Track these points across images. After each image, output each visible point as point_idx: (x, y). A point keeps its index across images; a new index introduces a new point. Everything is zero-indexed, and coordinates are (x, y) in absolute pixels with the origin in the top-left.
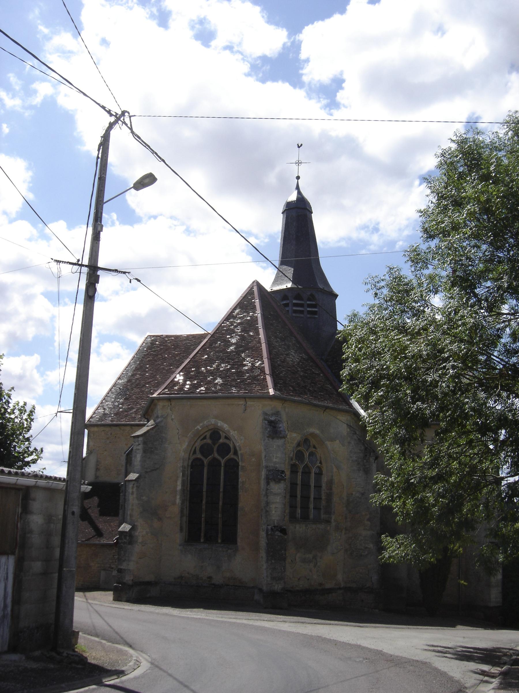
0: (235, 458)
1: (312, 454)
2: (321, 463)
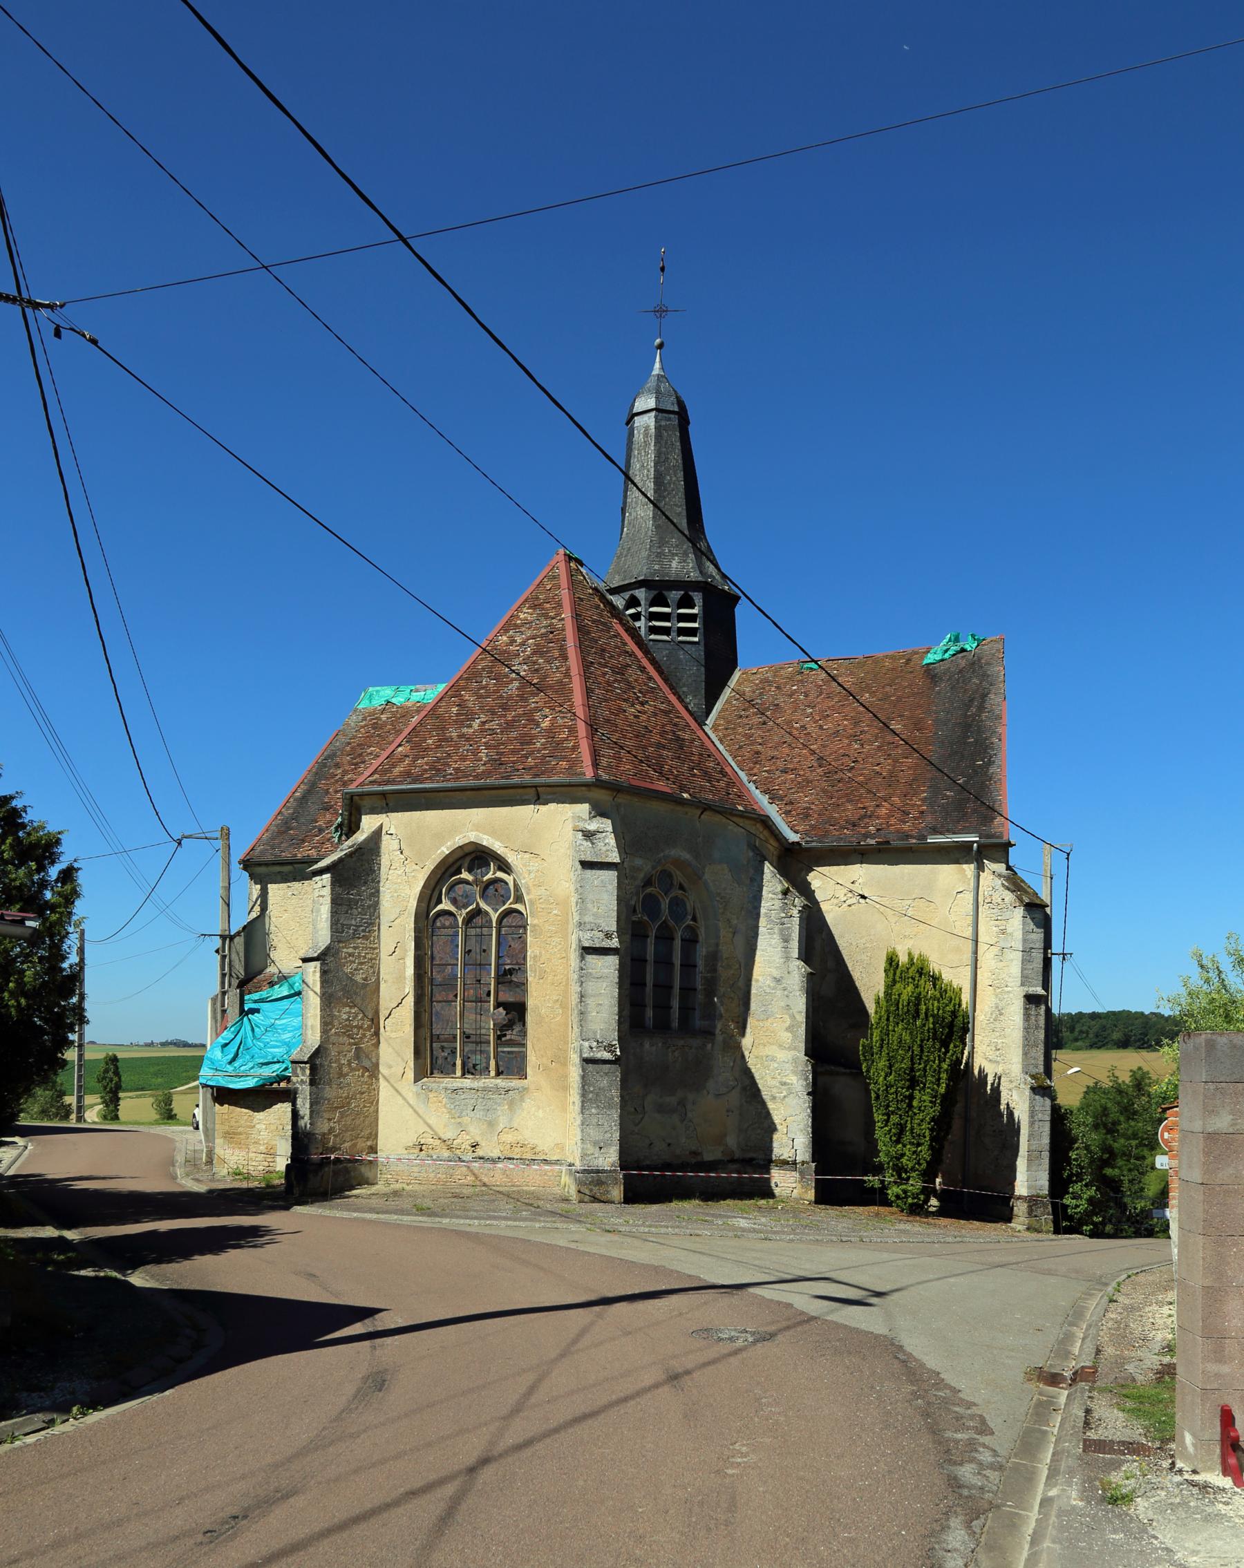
0: (518, 906)
1: (677, 904)
2: (694, 919)
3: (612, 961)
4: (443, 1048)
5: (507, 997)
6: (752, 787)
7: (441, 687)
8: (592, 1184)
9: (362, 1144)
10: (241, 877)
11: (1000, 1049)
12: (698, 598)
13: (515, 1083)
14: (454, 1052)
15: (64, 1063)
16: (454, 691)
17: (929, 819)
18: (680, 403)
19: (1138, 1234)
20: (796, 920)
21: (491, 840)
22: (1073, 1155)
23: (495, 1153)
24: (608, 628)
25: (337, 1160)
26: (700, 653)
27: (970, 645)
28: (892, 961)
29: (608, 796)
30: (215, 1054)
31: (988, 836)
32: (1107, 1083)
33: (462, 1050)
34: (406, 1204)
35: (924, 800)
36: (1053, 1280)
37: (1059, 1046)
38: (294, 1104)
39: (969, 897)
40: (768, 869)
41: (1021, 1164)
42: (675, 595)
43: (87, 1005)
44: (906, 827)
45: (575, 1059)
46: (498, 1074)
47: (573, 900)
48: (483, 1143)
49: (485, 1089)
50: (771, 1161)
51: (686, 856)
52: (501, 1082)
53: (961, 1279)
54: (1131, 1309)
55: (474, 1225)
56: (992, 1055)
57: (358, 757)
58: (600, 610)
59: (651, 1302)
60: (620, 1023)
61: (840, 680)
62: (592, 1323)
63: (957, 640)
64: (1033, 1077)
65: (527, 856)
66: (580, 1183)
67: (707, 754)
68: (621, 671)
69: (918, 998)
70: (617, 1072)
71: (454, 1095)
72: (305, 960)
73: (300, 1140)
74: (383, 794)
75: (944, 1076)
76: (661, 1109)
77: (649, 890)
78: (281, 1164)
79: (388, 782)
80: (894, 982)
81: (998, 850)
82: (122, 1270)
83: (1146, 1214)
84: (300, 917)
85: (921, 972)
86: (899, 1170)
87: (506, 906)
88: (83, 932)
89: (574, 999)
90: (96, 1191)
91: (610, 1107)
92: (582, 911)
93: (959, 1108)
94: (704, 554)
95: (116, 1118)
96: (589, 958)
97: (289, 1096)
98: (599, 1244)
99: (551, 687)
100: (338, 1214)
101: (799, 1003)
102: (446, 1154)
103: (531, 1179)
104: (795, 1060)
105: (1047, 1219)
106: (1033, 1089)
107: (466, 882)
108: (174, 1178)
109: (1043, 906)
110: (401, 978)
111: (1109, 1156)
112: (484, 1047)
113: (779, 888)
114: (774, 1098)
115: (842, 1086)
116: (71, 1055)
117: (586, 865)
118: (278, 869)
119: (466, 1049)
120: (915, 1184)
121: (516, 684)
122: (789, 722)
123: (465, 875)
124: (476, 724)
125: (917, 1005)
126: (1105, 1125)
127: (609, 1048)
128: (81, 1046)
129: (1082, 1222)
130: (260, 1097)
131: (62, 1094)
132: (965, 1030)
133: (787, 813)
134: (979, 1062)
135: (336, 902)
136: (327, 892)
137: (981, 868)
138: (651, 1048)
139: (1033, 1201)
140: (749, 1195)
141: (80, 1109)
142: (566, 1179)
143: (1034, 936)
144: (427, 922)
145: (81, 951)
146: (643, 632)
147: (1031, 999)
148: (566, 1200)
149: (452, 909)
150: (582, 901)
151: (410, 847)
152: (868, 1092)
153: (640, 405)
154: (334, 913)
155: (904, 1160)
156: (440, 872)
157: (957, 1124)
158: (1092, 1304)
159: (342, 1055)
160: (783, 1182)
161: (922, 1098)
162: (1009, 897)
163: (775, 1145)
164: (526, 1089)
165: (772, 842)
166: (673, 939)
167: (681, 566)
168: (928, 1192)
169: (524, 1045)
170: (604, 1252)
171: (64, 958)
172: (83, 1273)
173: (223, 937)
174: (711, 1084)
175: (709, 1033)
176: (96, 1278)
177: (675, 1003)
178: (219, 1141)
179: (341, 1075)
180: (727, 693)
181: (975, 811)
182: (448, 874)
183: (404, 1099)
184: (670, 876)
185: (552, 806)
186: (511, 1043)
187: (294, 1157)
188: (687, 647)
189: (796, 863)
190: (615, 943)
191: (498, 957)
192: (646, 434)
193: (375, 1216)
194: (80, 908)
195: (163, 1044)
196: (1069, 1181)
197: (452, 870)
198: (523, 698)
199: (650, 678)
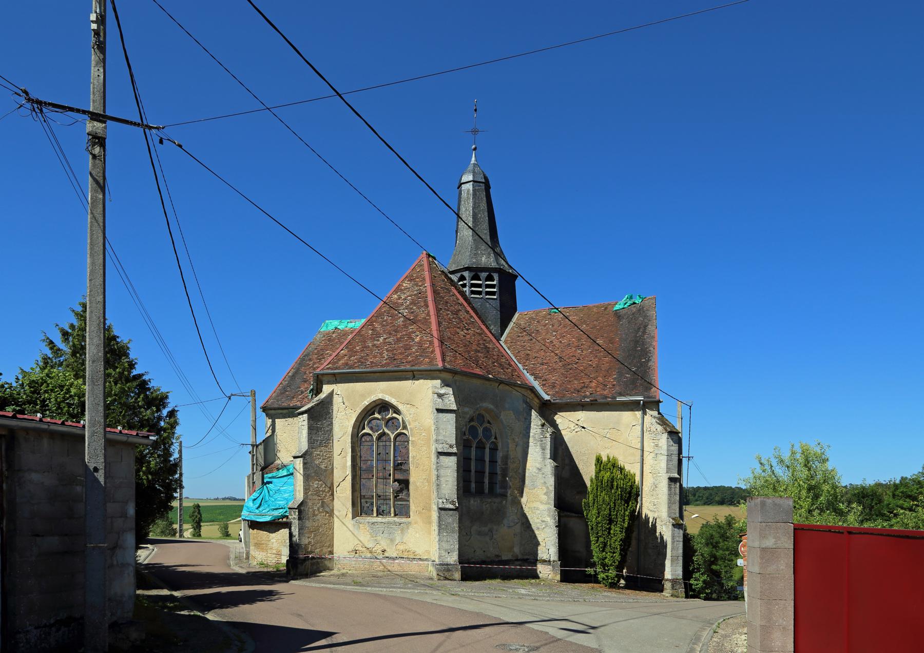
0: (404, 431)
1: (486, 430)
2: (496, 438)
3: (454, 459)
5: (399, 476)
6: (525, 372)
7: (363, 321)
8: (444, 571)
9: (325, 550)
10: (261, 415)
11: (656, 505)
12: (496, 276)
13: (404, 520)
14: (372, 504)
15: (172, 508)
16: (370, 322)
17: (617, 388)
18: (486, 178)
19: (729, 599)
20: (549, 439)
22: (695, 559)
23: (394, 555)
24: (449, 291)
25: (313, 558)
26: (497, 304)
27: (638, 301)
28: (599, 460)
29: (449, 376)
30: (249, 504)
31: (649, 397)
32: (713, 523)
34: (349, 580)
35: (615, 379)
36: (684, 621)
37: (687, 503)
38: (290, 530)
39: (639, 428)
40: (534, 414)
41: (668, 563)
42: (484, 275)
43: (184, 479)
44: (605, 392)
45: (435, 508)
46: (396, 515)
47: (433, 428)
48: (388, 550)
49: (388, 523)
50: (537, 560)
51: (491, 407)
52: (396, 519)
53: (637, 620)
54: (725, 636)
55: (384, 591)
56: (652, 508)
57: (321, 356)
58: (446, 282)
59: (477, 630)
60: (458, 490)
61: (571, 318)
62: (445, 641)
63: (631, 298)
64: (673, 519)
66: (438, 570)
67: (501, 355)
68: (456, 313)
69: (613, 479)
70: (456, 515)
72: (295, 457)
73: (294, 548)
74: (334, 374)
75: (627, 518)
76: (480, 533)
77: (472, 424)
78: (284, 559)
79: (336, 368)
80: (600, 470)
81: (655, 404)
82: (203, 611)
83: (733, 589)
84: (292, 436)
85: (614, 466)
86: (604, 565)
88: (181, 443)
89: (434, 478)
90: (189, 572)
91: (453, 532)
92: (438, 434)
93: (635, 535)
94: (499, 255)
95: (200, 535)
96: (441, 457)
97: (288, 525)
98: (448, 601)
99: (420, 321)
100: (314, 585)
101: (551, 481)
102: (369, 555)
103: (413, 568)
104: (549, 510)
105: (681, 591)
106: (673, 525)
107: (378, 419)
108: (229, 566)
109: (677, 433)
110: (344, 467)
111: (714, 560)
113: (540, 423)
114: (538, 528)
115: (574, 523)
116: (176, 504)
117: (439, 411)
118: (280, 411)
120: (612, 573)
121: (402, 319)
122: (544, 339)
123: (377, 415)
124: (381, 339)
125: (612, 482)
126: (712, 544)
127: (452, 503)
128: (181, 499)
129: (700, 592)
130: (273, 526)
131: (172, 523)
132: (638, 495)
133: (544, 385)
134: (645, 511)
135: (310, 428)
136: (306, 423)
137: (645, 413)
138: (474, 503)
139: (674, 582)
140: (527, 578)
141: (181, 531)
142: (431, 568)
143: (673, 448)
144: (357, 439)
145: (180, 452)
146: (467, 294)
147: (671, 480)
148: (431, 579)
149: (370, 432)
150: (437, 428)
151: (348, 402)
152: (587, 526)
153: (464, 179)
154: (309, 434)
155: (606, 561)
157: (634, 542)
158: (705, 634)
159: (314, 505)
160: (543, 570)
161: (615, 529)
162: (660, 428)
163: (539, 552)
164: (410, 523)
165: (536, 399)
166: (484, 448)
167: (487, 260)
168: (619, 577)
169: (408, 501)
170: (451, 605)
171: (171, 455)
172: (182, 613)
173: (253, 446)
174: (505, 522)
175: (504, 496)
176: (189, 615)
177: (486, 480)
178: (252, 548)
179: (314, 515)
180: (511, 325)
181: (641, 385)
184: (483, 416)
185: (421, 381)
187: (290, 556)
188: (490, 301)
189: (548, 410)
190: (455, 450)
191: (395, 457)
192: (468, 193)
193: (332, 586)
194: (178, 430)
195: (223, 499)
196: (693, 572)
198: (405, 326)
199: (472, 317)
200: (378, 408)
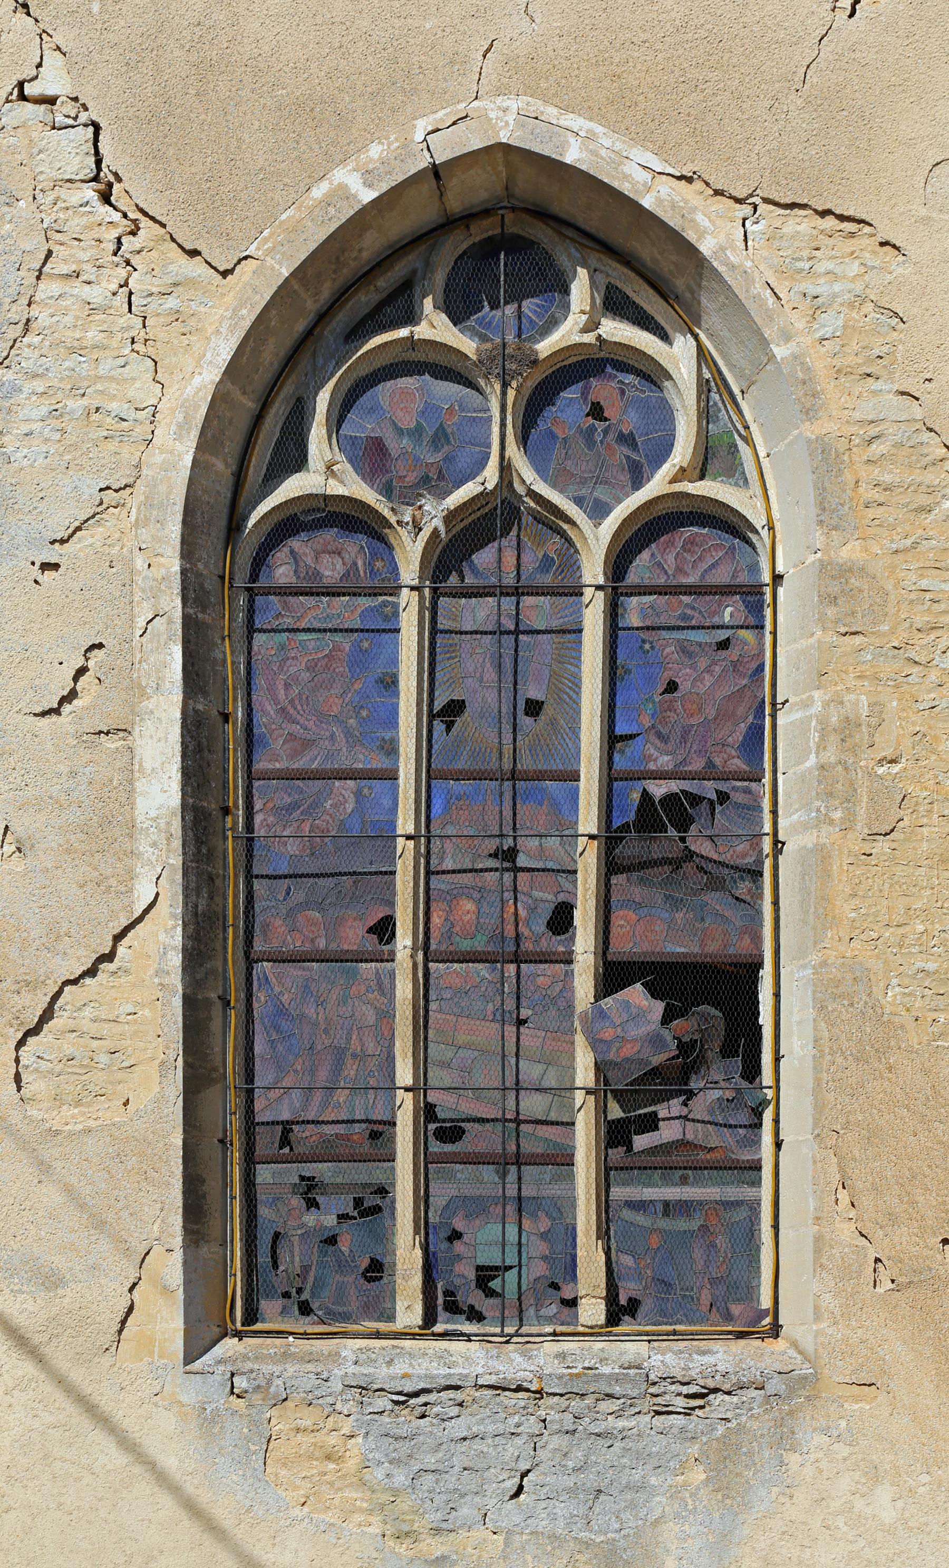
4: (310, 1192)
5: (664, 930)
13: (722, 1357)
14: (372, 1207)
21: (607, 140)
33: (423, 1199)
49: (580, 1389)
65: (801, 225)
71: (406, 1421)
87: (657, 484)
107: (442, 366)
112: (536, 1182)
119: (441, 1194)
123: (434, 326)
156: (312, 306)
182: (342, 319)
183: (128, 1445)
186: (679, 1161)
191: (613, 740)
197: (366, 299)
200: (455, 245)
